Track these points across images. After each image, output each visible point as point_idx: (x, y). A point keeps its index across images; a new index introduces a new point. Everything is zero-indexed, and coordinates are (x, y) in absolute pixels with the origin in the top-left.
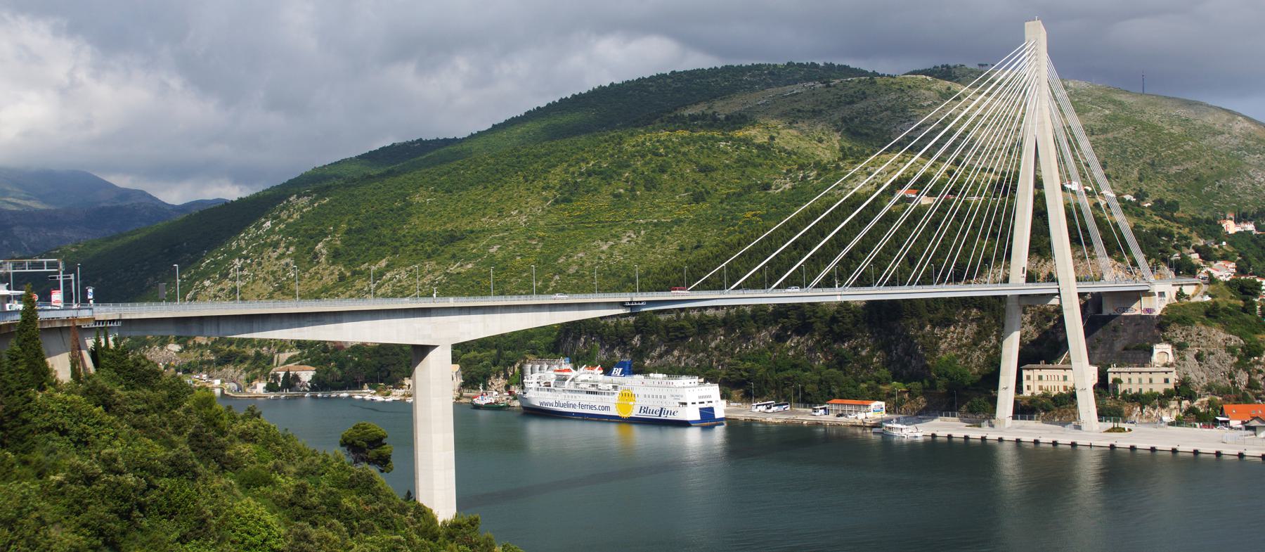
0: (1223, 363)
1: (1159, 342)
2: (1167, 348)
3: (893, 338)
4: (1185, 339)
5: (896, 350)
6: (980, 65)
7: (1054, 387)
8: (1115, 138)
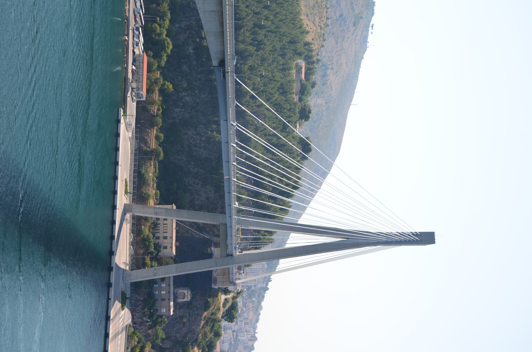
0: (177, 332)
1: (192, 292)
2: (188, 297)
3: (197, 91)
4: (194, 307)
5: (187, 96)
6: (373, 25)
7: (159, 230)
8: (323, 115)
